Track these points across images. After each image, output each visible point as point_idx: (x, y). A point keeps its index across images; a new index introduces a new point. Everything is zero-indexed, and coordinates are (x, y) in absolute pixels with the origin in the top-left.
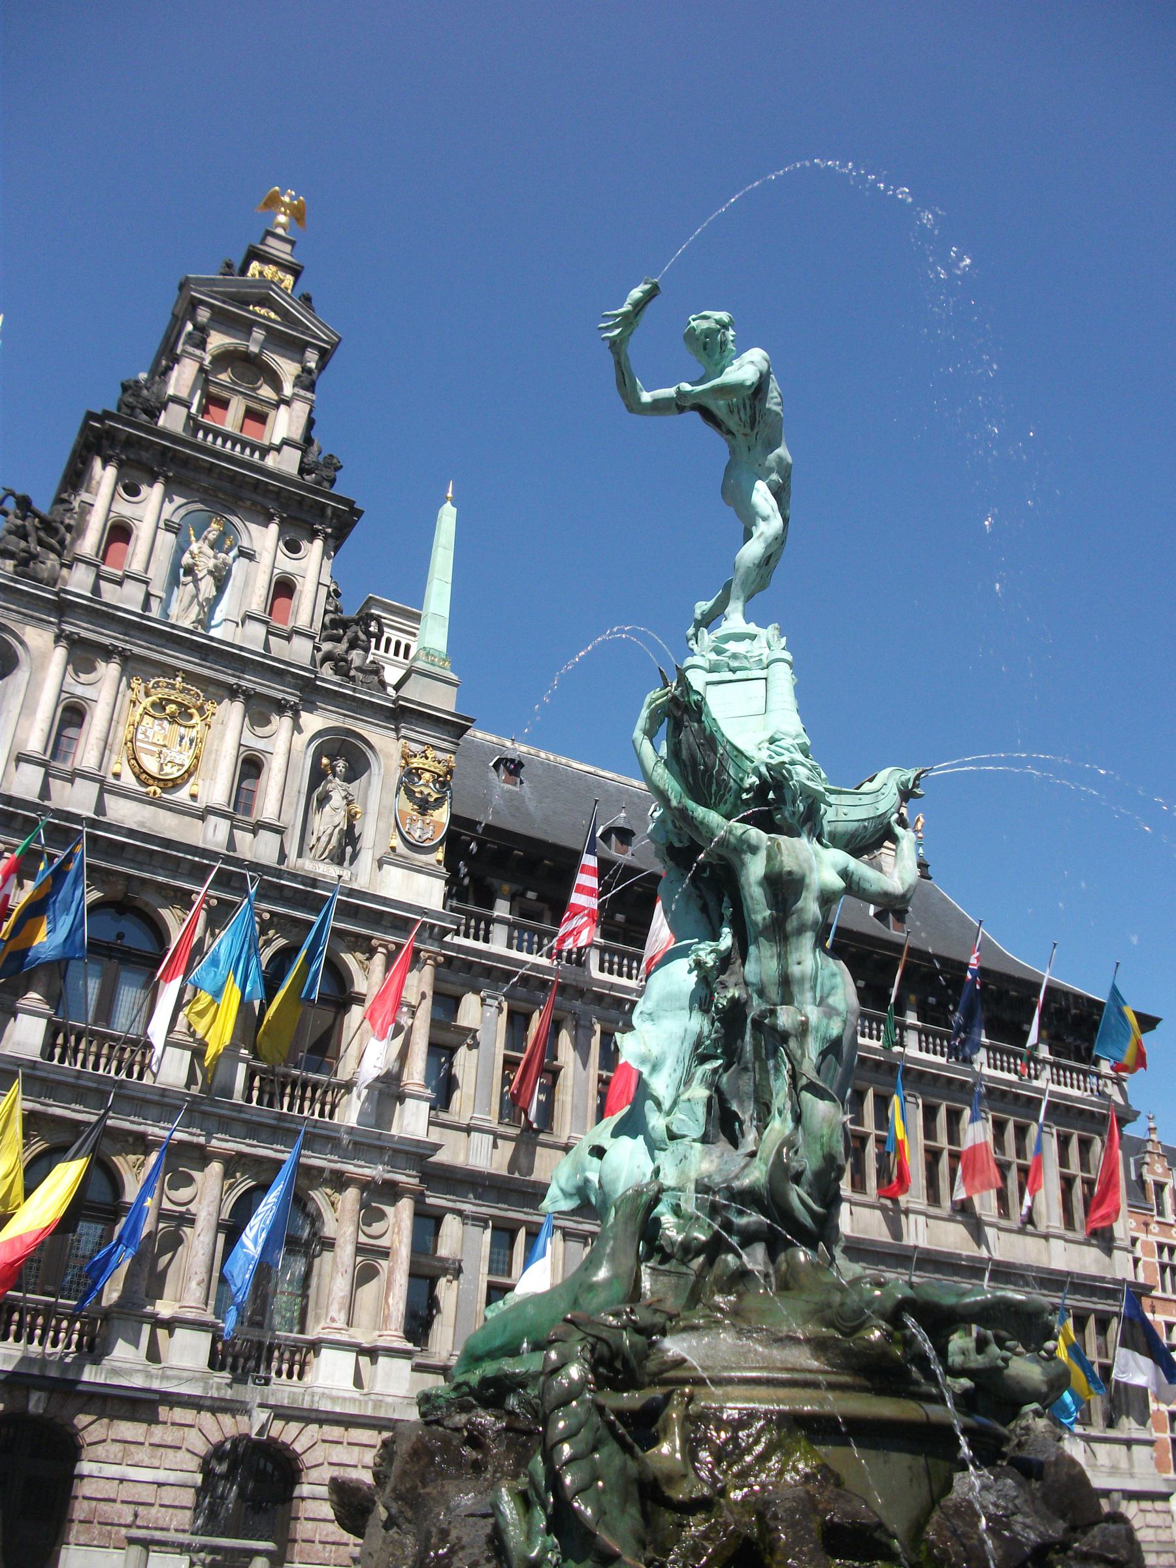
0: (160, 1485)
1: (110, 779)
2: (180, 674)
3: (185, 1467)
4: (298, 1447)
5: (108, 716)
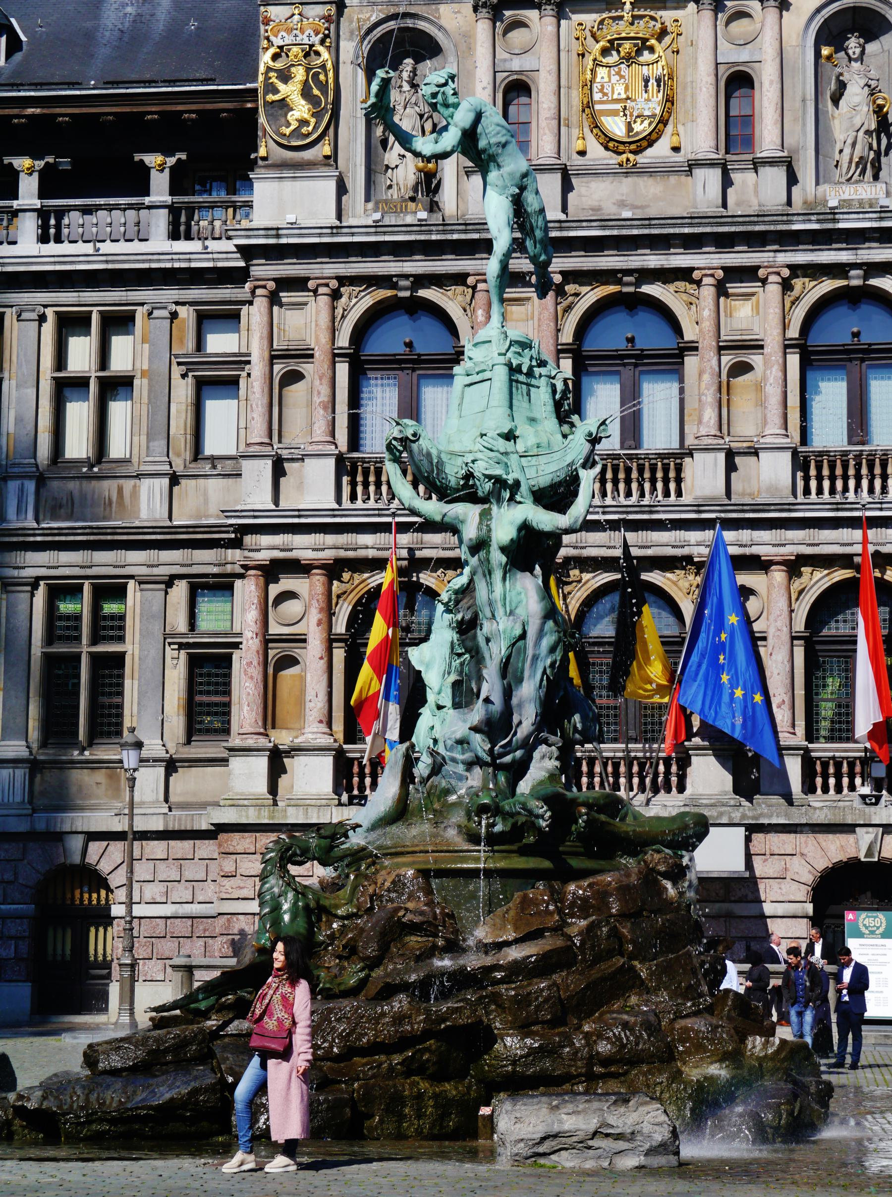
1: (578, 160)
3: (792, 898)
5: (554, 86)
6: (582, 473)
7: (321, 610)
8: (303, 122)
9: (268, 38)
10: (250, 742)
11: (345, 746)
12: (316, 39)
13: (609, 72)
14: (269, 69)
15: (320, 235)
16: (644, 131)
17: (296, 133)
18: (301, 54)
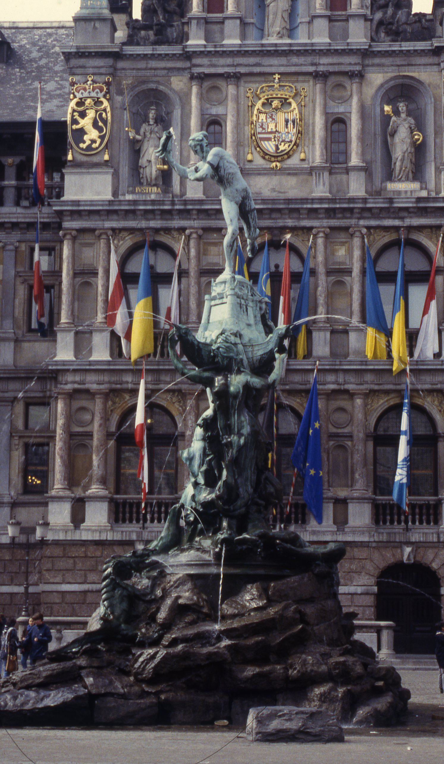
0: (352, 594)
2: (277, 76)
4: (435, 566)
6: (277, 355)
7: (102, 418)
8: (93, 141)
9: (73, 93)
10: (61, 494)
11: (115, 496)
12: (100, 95)
13: (266, 117)
14: (74, 111)
15: (102, 205)
16: (285, 150)
17: (89, 148)
18: (93, 103)
